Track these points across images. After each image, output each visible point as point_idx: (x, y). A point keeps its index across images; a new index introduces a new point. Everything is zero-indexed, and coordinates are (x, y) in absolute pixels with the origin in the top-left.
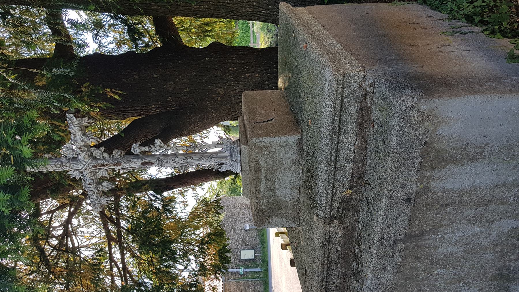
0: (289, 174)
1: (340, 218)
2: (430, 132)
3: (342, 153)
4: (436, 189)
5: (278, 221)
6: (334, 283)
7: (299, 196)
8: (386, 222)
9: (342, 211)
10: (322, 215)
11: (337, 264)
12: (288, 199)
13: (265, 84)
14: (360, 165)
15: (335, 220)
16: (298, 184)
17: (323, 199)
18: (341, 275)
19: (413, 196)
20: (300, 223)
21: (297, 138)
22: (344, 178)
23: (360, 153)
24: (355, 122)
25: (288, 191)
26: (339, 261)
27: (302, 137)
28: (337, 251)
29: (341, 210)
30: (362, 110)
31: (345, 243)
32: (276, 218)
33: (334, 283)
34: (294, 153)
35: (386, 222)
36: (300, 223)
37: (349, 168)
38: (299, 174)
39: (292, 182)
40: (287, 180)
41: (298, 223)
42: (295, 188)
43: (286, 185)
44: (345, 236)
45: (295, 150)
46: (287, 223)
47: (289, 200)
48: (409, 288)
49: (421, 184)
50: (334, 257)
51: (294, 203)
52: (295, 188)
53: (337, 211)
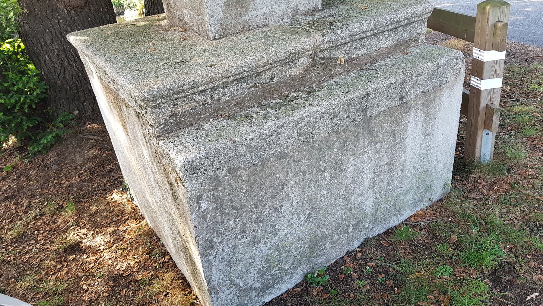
0: (283, 7)
1: (313, 65)
2: (448, 84)
3: (375, 39)
4: (408, 116)
5: (219, 9)
6: (225, 94)
7: (255, 27)
8: (385, 89)
9: (322, 63)
10: (326, 40)
11: (255, 86)
12: (252, 13)
13: (89, 6)
14: (369, 60)
15: (311, 60)
16: (270, 21)
17: (343, 34)
18: (241, 98)
19: (405, 100)
20: (219, 39)
21: (319, 7)
22: (354, 51)
23: (378, 55)
24: (397, 41)
25: (261, 12)
26: (258, 86)
27: (320, 11)
28: (272, 79)
29: (322, 62)
30: (407, 42)
31: (285, 83)
32: (223, 5)
33: (225, 94)
34: (305, 7)
35: (385, 89)
36: (219, 39)
37: (363, 51)
38: (282, 20)
39: (273, 13)
40: (276, 7)
41: (217, 37)
42: (266, 19)
43: (270, 7)
44: (294, 79)
45: (308, 7)
46: (216, 22)
47: (250, 15)
48: (308, 159)
49: (414, 101)
50: (264, 78)
51: (245, 24)
52: (266, 19)
53: (322, 58)
